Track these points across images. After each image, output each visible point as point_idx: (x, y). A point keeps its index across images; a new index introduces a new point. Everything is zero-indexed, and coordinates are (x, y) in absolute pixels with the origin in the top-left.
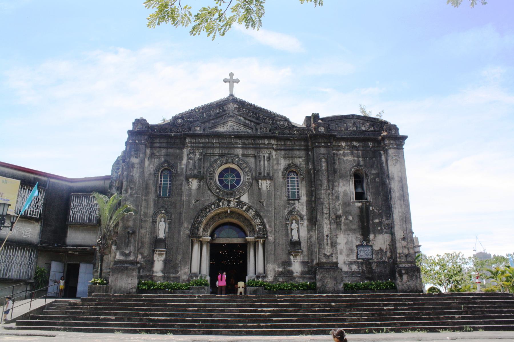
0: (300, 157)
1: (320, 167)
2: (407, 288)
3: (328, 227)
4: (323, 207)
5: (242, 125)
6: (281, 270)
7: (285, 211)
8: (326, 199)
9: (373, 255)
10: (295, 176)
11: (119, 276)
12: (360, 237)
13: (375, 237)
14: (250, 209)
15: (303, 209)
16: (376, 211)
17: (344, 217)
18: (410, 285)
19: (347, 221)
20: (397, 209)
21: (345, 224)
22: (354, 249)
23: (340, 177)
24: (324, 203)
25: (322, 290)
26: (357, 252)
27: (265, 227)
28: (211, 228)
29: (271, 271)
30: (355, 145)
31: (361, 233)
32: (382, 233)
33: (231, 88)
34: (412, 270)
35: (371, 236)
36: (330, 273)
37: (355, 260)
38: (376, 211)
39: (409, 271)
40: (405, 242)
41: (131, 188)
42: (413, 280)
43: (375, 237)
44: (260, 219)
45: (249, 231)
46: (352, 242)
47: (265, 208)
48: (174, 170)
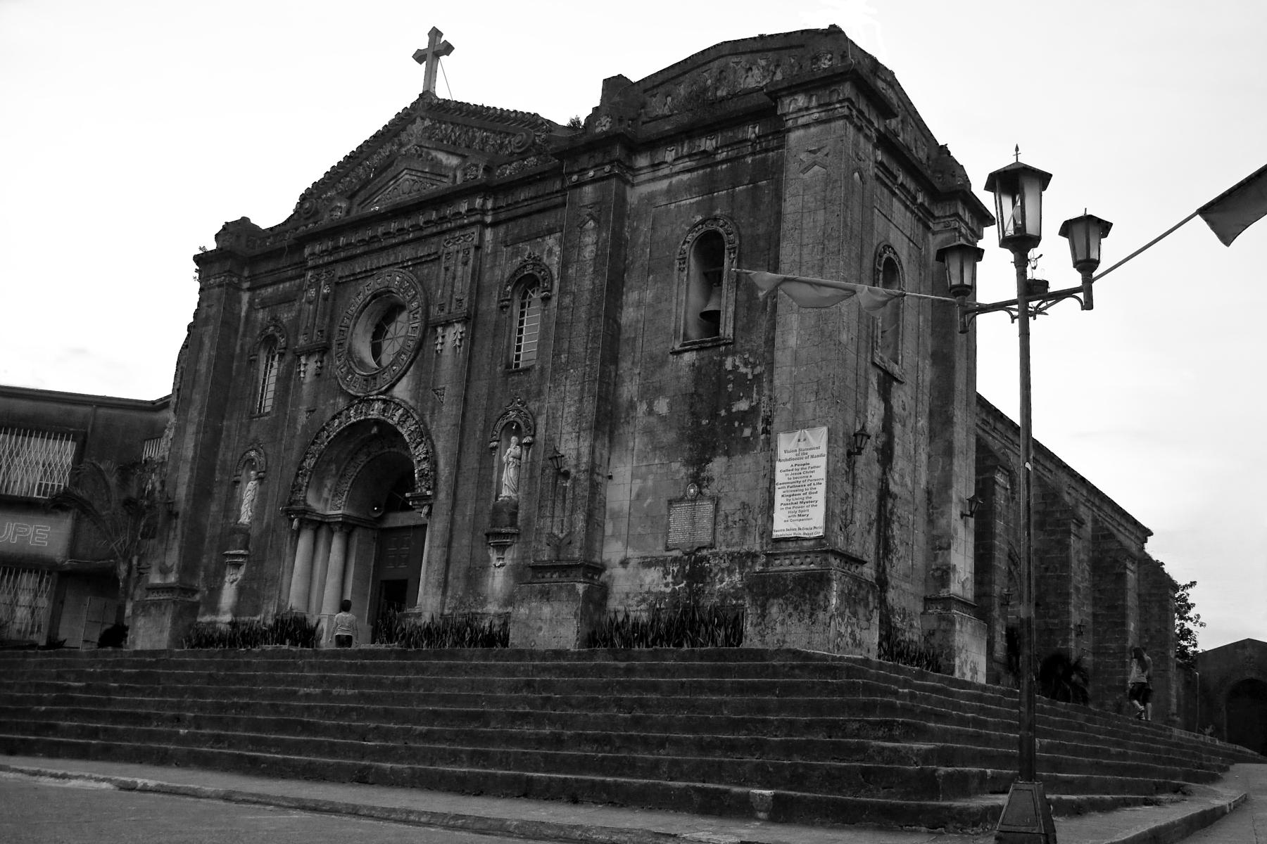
33: (430, 76)
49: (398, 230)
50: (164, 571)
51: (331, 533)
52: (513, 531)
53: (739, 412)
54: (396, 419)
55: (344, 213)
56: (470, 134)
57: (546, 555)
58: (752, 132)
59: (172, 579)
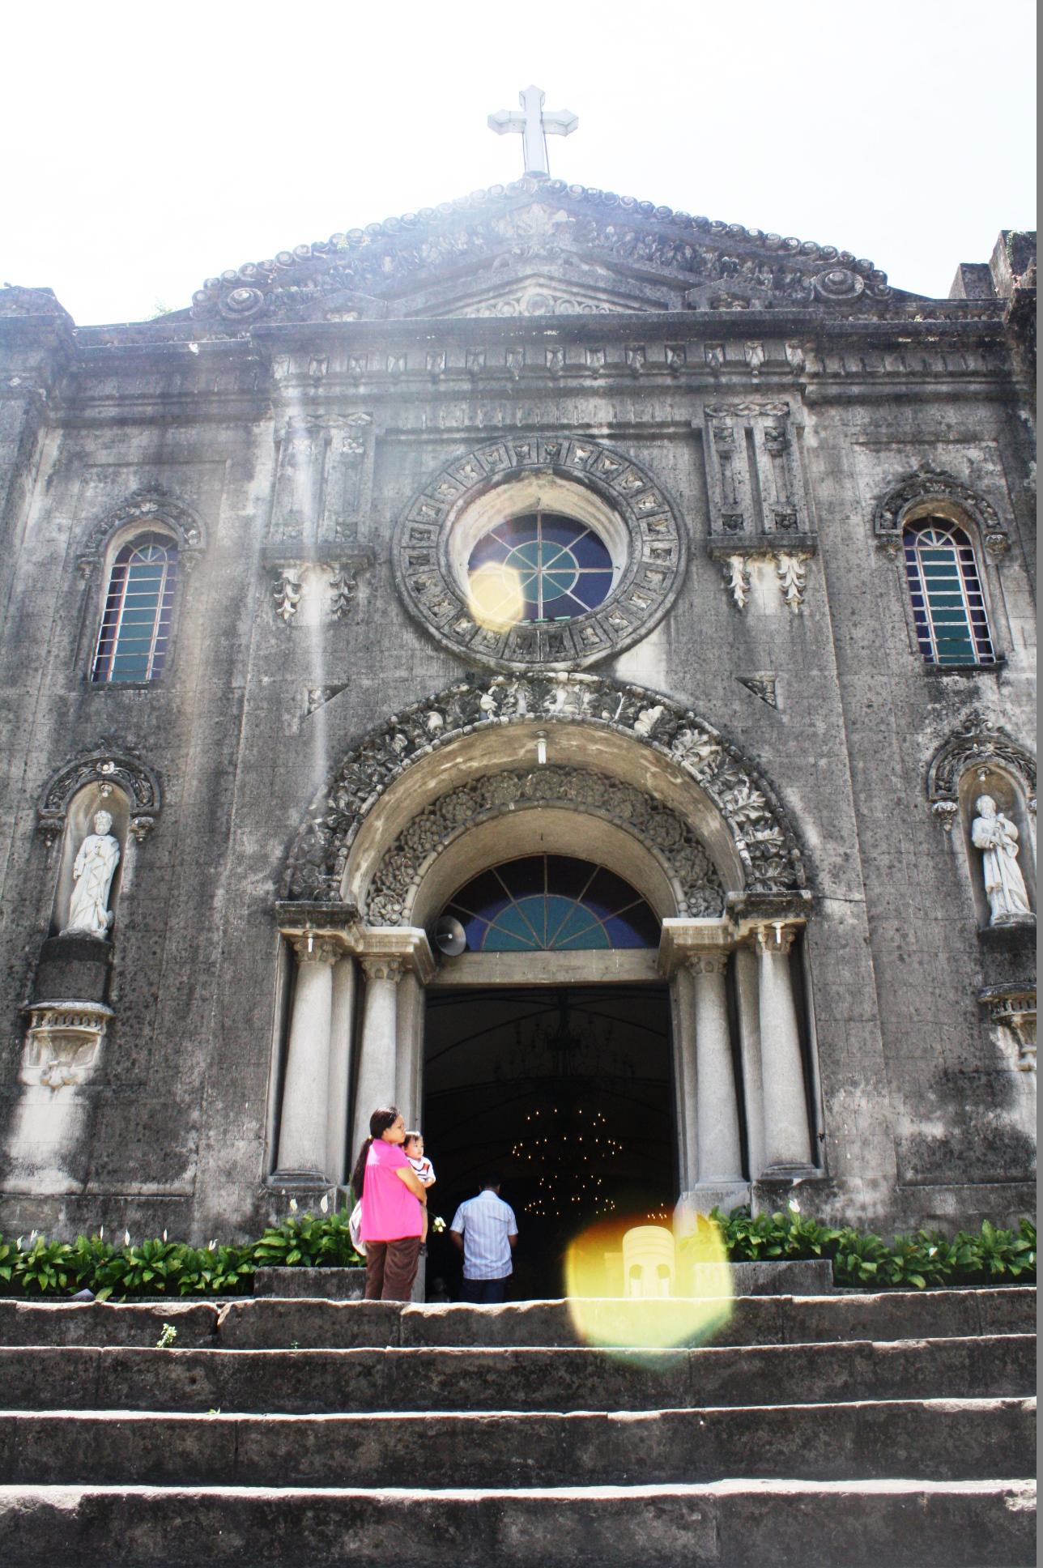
6: (936, 1130)
10: (948, 542)
14: (681, 727)
27: (793, 835)
28: (422, 871)
29: (865, 1143)
44: (755, 786)
45: (683, 885)
47: (785, 719)
48: (193, 532)
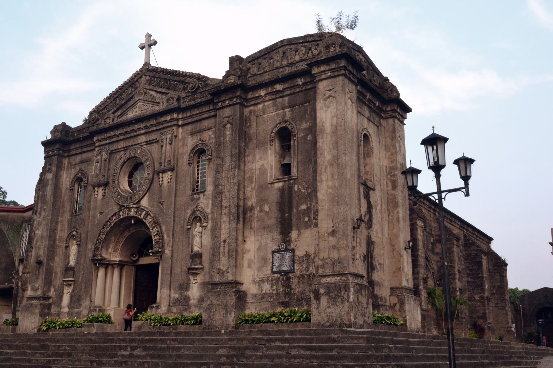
0: (209, 129)
1: (222, 138)
2: (326, 319)
3: (226, 227)
4: (223, 198)
5: (150, 103)
6: (177, 296)
7: (188, 211)
8: (227, 185)
9: (296, 265)
11: (26, 314)
12: (278, 237)
13: (299, 235)
15: (208, 204)
16: (303, 191)
17: (258, 208)
18: (331, 314)
19: (262, 214)
20: (324, 184)
21: (260, 220)
22: (269, 257)
23: (257, 146)
24: (224, 192)
25: (207, 324)
26: (273, 261)
29: (165, 299)
30: (278, 89)
31: (279, 230)
32: (310, 227)
33: (148, 56)
34: (336, 287)
35: (294, 234)
36: (219, 298)
37: (269, 276)
38: (303, 191)
39: (332, 290)
40: (335, 239)
41: (45, 210)
42: (337, 306)
43: (299, 235)
46: (266, 245)
49: (138, 129)
50: (36, 290)
51: (114, 268)
52: (201, 267)
53: (302, 210)
54: (142, 216)
55: (111, 121)
56: (169, 83)
57: (217, 279)
58: (300, 82)
59: (39, 293)
